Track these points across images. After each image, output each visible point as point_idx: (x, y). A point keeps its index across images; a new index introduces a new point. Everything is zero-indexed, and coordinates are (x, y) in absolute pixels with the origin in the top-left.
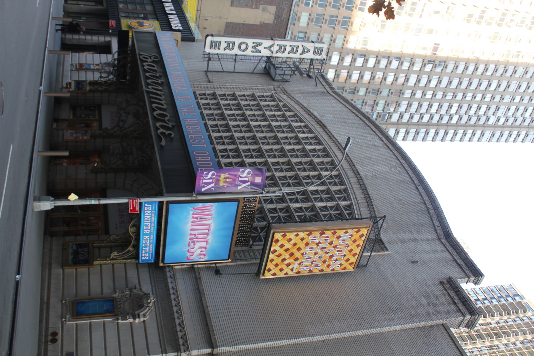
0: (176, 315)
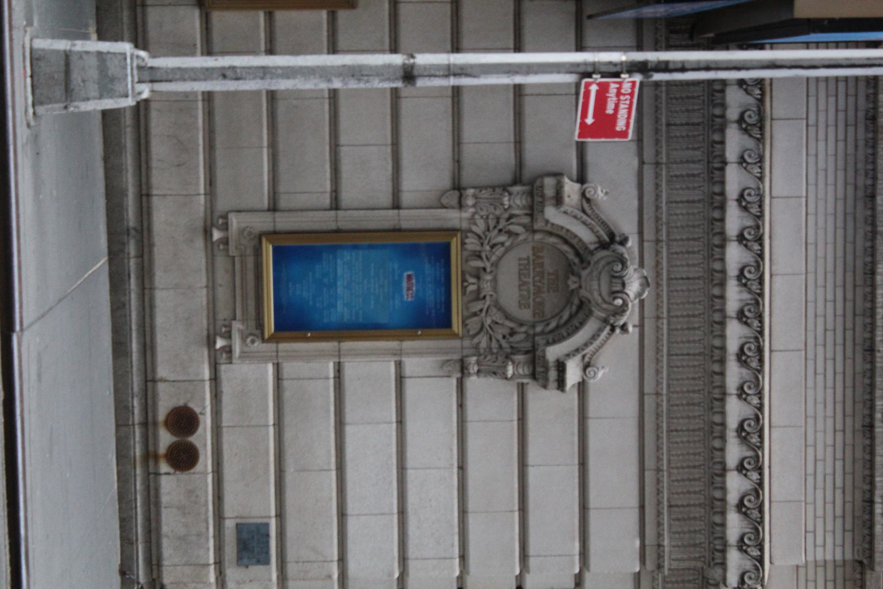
0: (734, 374)
